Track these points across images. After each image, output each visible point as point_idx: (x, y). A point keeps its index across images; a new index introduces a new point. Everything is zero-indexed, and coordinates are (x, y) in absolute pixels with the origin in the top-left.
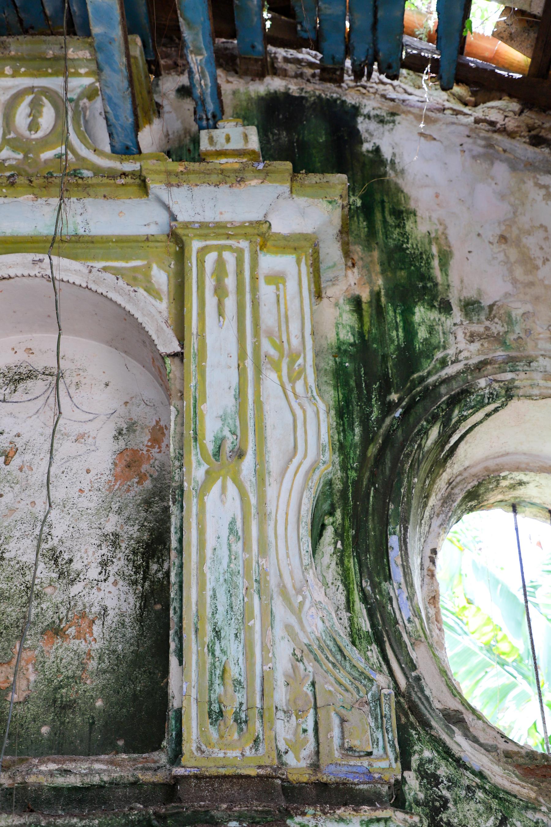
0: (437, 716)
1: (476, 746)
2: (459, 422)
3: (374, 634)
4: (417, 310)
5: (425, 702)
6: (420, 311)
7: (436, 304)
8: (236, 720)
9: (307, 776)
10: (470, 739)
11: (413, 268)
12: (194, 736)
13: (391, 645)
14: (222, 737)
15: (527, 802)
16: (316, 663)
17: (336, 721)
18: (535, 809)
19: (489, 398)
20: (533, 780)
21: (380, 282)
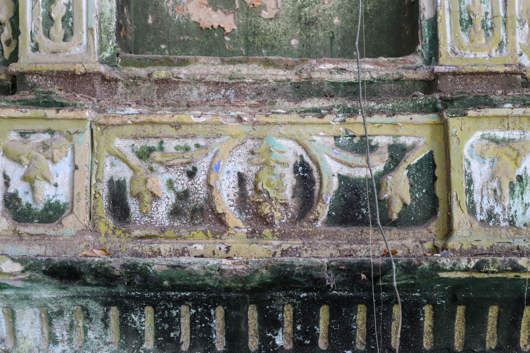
12: (449, 41)
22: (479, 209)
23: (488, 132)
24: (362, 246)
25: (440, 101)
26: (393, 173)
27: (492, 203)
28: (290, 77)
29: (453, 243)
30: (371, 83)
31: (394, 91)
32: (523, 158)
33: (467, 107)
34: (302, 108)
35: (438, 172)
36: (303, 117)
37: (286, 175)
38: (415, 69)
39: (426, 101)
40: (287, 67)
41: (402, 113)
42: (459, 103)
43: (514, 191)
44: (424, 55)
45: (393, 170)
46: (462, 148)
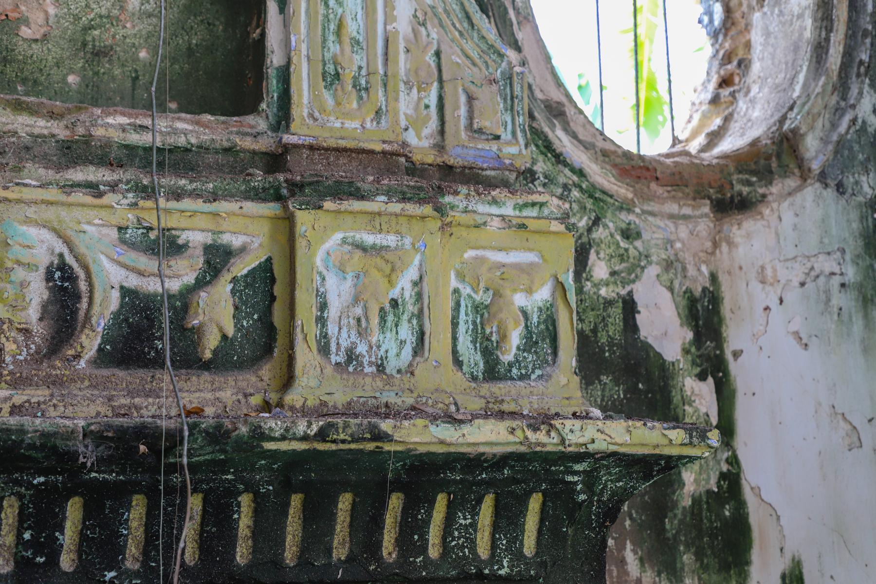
0: (539, 106)
8: (354, 86)
9: (432, 156)
10: (569, 135)
12: (305, 100)
14: (338, 104)
15: (622, 203)
17: (463, 99)
18: (629, 211)
20: (628, 180)
22: (335, 347)
23: (352, 234)
24: (150, 400)
25: (284, 185)
26: (209, 288)
27: (353, 338)
28: (56, 131)
29: (293, 397)
30: (187, 150)
31: (223, 165)
32: (400, 275)
33: (323, 196)
34: (67, 180)
35: (278, 290)
36: (69, 194)
37: (32, 284)
38: (255, 137)
39: (265, 183)
40: (52, 115)
41: (228, 198)
42: (312, 189)
43: (385, 321)
44: (270, 118)
45: (209, 282)
46: (314, 255)
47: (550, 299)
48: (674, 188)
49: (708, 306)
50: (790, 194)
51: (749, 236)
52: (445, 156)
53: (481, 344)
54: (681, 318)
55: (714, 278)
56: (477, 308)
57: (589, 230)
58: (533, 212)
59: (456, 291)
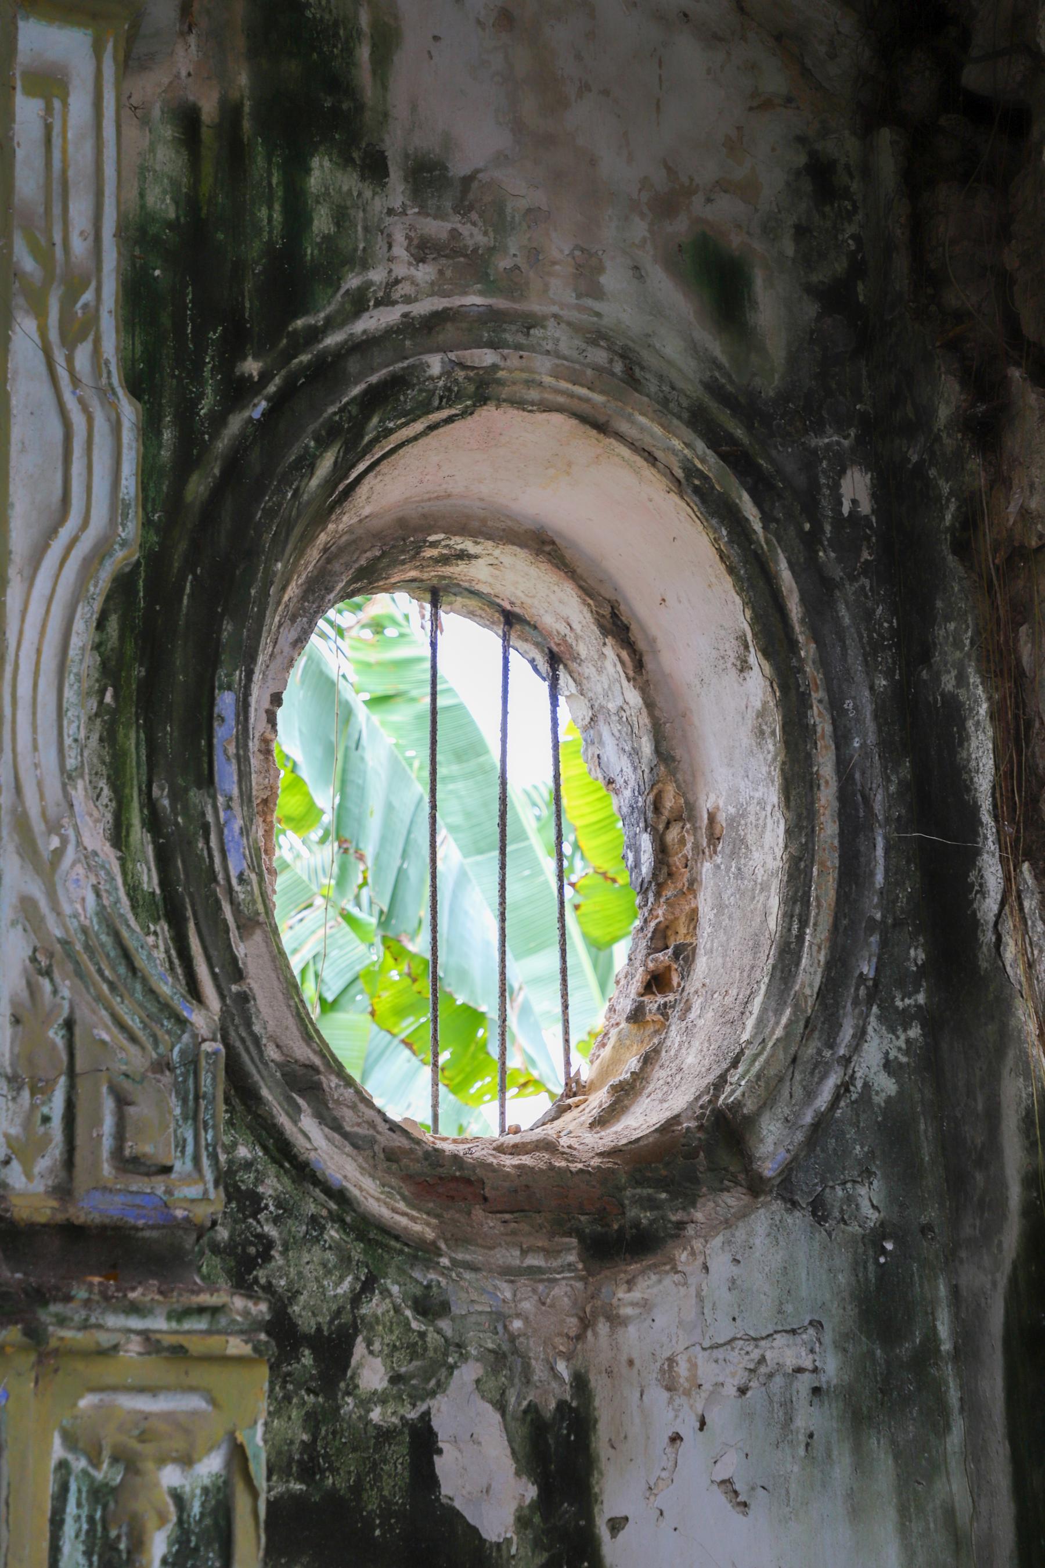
0: (272, 1076)
1: (337, 1137)
2: (376, 440)
3: (165, 899)
4: (315, 162)
5: (252, 1048)
6: (322, 166)
7: (355, 155)
10: (326, 1125)
11: (315, 55)
13: (197, 924)
15: (417, 1249)
16: (78, 982)
17: (109, 1105)
18: (430, 1264)
19: (441, 398)
20: (431, 1205)
21: (243, 79)
47: (223, 1473)
48: (516, 1215)
49: (569, 1435)
50: (727, 1224)
51: (645, 1305)
52: (72, 1210)
53: (100, 1557)
54: (517, 1460)
55: (580, 1383)
56: (99, 1494)
57: (356, 1300)
58: (201, 1324)
59: (63, 1465)
